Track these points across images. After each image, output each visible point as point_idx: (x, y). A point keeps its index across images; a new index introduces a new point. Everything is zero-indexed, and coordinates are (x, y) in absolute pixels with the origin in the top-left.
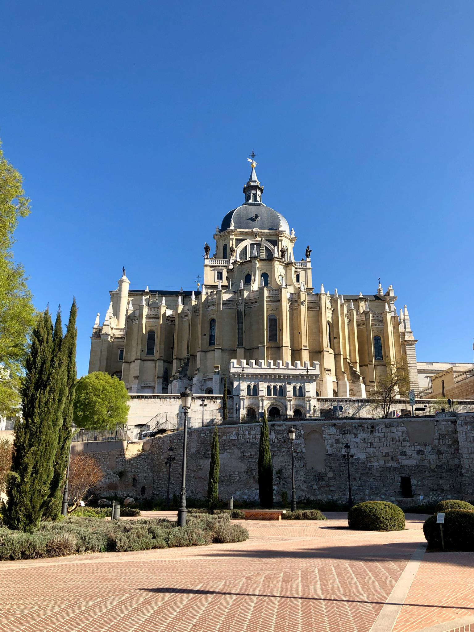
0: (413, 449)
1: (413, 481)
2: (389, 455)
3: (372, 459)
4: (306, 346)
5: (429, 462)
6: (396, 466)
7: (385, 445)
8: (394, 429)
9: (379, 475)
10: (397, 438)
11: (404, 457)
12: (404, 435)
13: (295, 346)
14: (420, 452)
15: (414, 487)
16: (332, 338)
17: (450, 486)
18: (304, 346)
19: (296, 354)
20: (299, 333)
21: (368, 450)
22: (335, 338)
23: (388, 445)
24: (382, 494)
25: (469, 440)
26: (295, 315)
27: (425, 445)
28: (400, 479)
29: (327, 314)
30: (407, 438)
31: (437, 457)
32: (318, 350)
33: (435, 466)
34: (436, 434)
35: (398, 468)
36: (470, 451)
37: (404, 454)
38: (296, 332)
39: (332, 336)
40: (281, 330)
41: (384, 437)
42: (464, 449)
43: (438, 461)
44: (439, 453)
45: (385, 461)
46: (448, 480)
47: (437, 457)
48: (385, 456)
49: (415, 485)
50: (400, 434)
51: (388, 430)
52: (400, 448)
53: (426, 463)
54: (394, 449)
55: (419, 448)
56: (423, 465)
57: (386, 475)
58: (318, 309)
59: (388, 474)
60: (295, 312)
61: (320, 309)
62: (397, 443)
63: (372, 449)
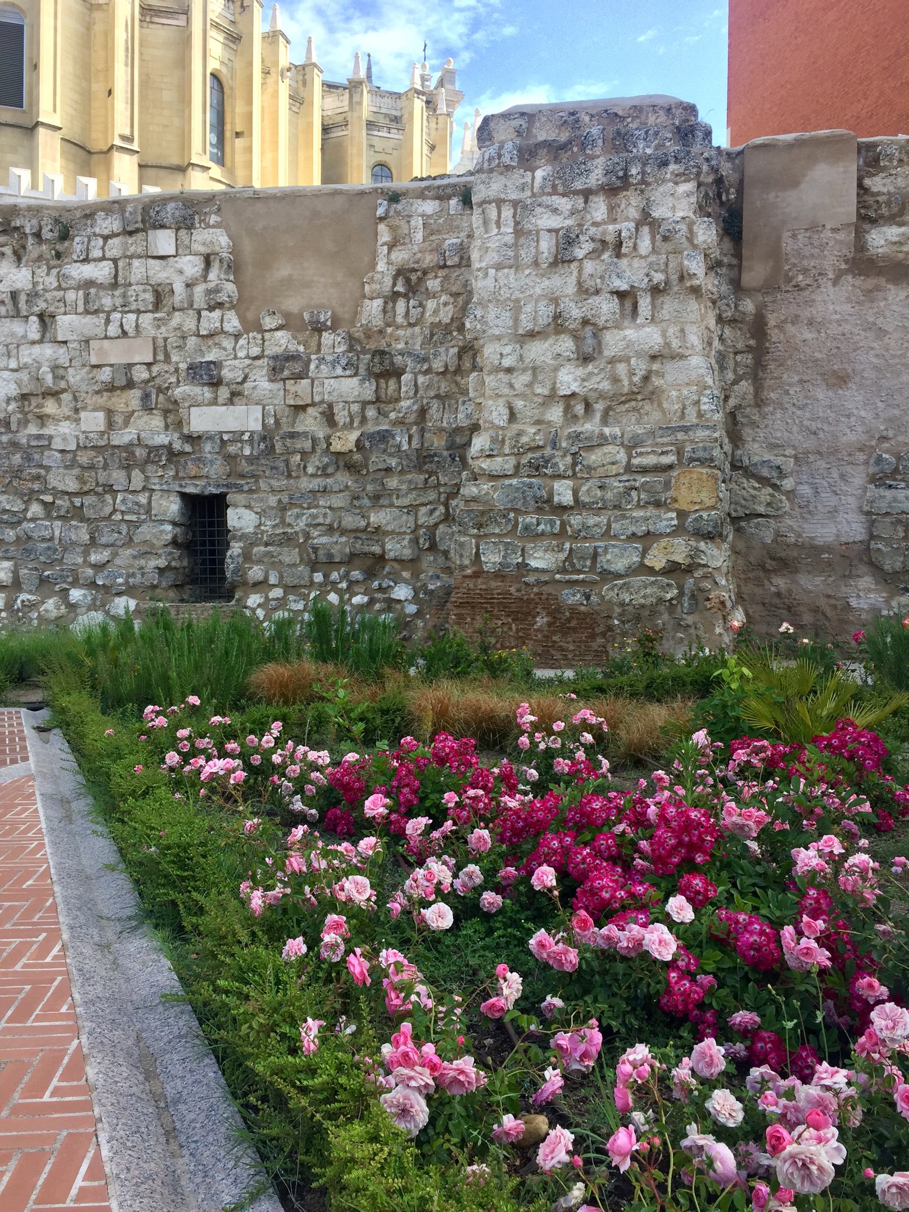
0: (255, 351)
1: (240, 518)
2: (130, 384)
3: (50, 407)
4: (130, 139)
5: (329, 418)
6: (162, 439)
7: (113, 330)
8: (164, 242)
9: (72, 485)
10: (179, 287)
11: (207, 393)
12: (212, 276)
13: (94, 136)
14: (284, 367)
15: (236, 548)
16: (228, 134)
17: (416, 541)
18: (123, 138)
19: (87, 155)
20: (110, 92)
21: (27, 355)
22: (238, 135)
23: (129, 328)
24: (75, 583)
25: (527, 255)
26: (98, 28)
27: (318, 329)
28: (173, 507)
29: (211, 44)
30: (230, 287)
31: (368, 391)
32: (175, 161)
33: (354, 436)
34: (381, 266)
35: (169, 448)
36: (526, 324)
37: (208, 375)
38: (98, 88)
39: (228, 127)
40: (36, 67)
41: (115, 285)
42: (492, 311)
43: (371, 413)
44: (385, 370)
45: (110, 413)
46: (412, 509)
47: (368, 391)
48: (111, 388)
49: (243, 537)
50: (191, 266)
51: (135, 244)
52: (192, 341)
53: (311, 423)
54: (161, 351)
55: (282, 341)
56: (293, 435)
57: (110, 489)
58: (181, 21)
59: (118, 477)
60: (98, 15)
61: (188, 21)
62: (177, 318)
63: (48, 351)
